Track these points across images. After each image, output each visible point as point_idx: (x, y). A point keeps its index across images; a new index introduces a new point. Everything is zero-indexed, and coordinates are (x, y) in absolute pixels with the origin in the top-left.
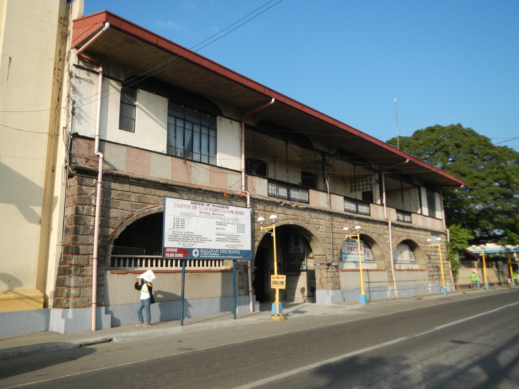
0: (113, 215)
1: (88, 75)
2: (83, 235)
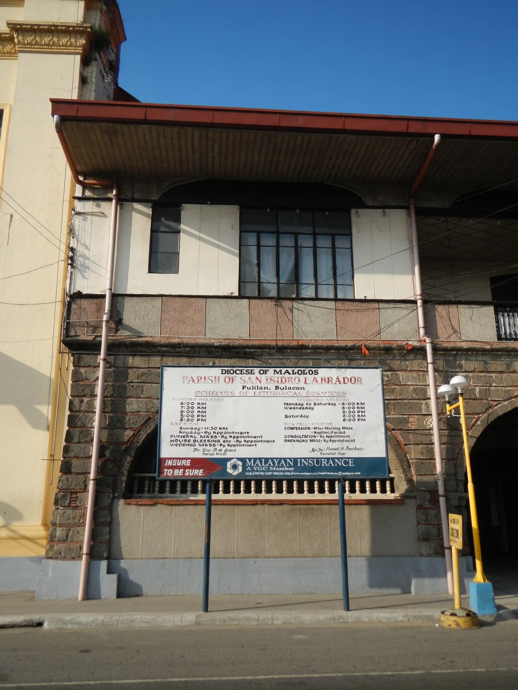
0: (131, 408)
1: (98, 206)
2: (78, 443)
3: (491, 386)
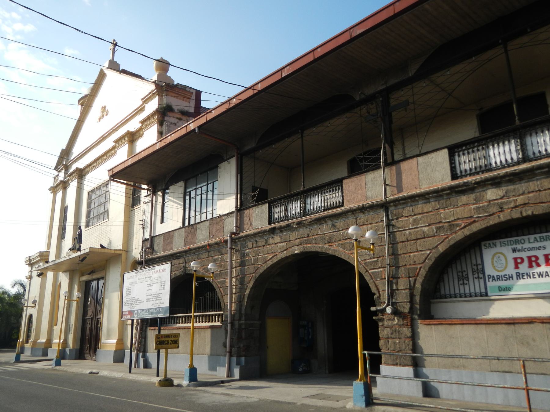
3: (258, 256)
